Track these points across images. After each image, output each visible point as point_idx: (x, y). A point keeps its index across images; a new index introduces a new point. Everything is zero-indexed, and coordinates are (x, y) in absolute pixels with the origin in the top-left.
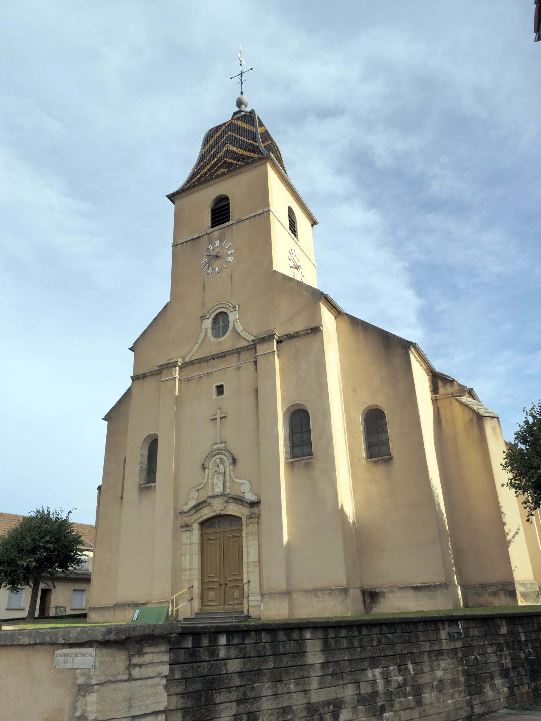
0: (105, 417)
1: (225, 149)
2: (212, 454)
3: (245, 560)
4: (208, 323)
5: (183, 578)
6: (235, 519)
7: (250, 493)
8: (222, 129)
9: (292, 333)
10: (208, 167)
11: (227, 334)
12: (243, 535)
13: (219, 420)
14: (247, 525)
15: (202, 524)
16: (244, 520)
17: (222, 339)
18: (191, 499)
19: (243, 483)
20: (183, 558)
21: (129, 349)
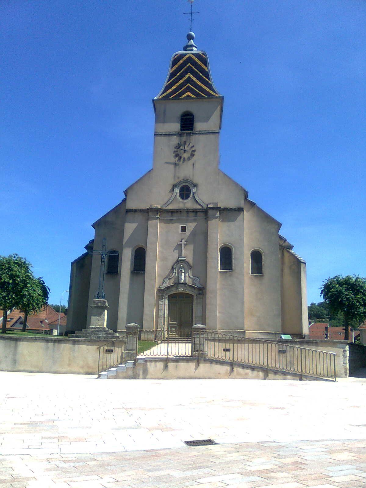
0: (93, 224)
1: (187, 76)
2: (177, 262)
3: (194, 315)
4: (177, 190)
5: (159, 321)
6: (190, 297)
7: (199, 284)
8: (185, 58)
9: (228, 208)
10: (176, 86)
11: (189, 199)
12: (194, 303)
13: (183, 245)
14: (197, 299)
15: (169, 296)
16: (195, 297)
17: (186, 201)
18: (164, 282)
19: (195, 279)
20: (159, 311)
21: (123, 191)
